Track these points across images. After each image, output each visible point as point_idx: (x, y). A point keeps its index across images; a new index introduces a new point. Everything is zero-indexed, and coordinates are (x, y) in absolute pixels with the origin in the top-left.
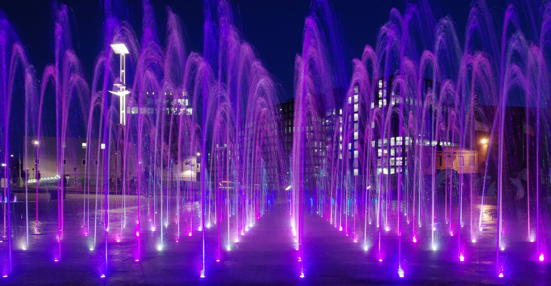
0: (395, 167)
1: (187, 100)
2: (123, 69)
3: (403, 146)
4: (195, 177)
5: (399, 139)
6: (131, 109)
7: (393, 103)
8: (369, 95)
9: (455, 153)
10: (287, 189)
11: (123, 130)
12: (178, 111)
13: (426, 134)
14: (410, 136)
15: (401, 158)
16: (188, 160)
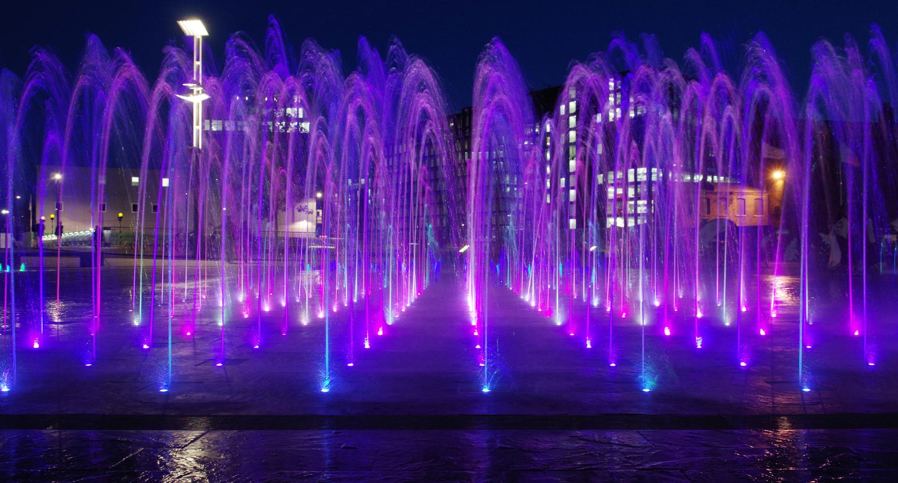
0: (636, 216)
1: (301, 110)
2: (198, 60)
3: (650, 183)
4: (314, 231)
5: (642, 171)
6: (211, 122)
7: (632, 115)
8: (591, 104)
9: (731, 193)
10: (462, 251)
12: (286, 127)
13: (685, 164)
14: (661, 167)
16: (303, 205)
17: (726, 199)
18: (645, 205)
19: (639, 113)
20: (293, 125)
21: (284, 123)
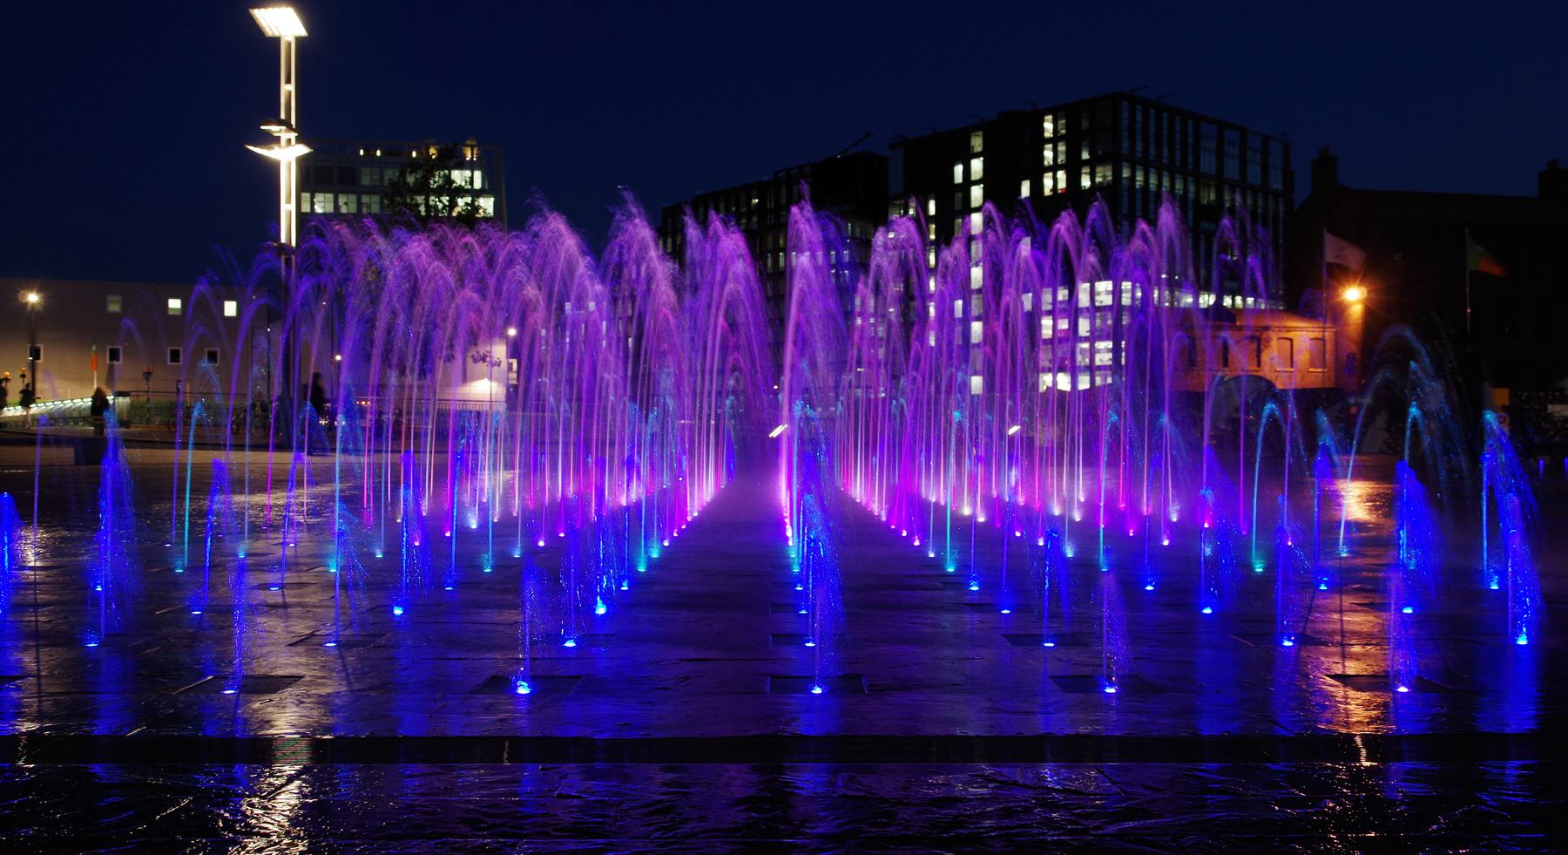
0: (1092, 369)
1: (478, 175)
2: (288, 81)
3: (1117, 308)
5: (1104, 286)
6: (312, 197)
9: (1267, 328)
10: (775, 434)
11: (288, 261)
12: (453, 204)
15: (1110, 344)
16: (482, 349)
17: (1259, 340)
18: (1108, 351)
19: (1098, 180)
20: (461, 202)
21: (445, 199)
